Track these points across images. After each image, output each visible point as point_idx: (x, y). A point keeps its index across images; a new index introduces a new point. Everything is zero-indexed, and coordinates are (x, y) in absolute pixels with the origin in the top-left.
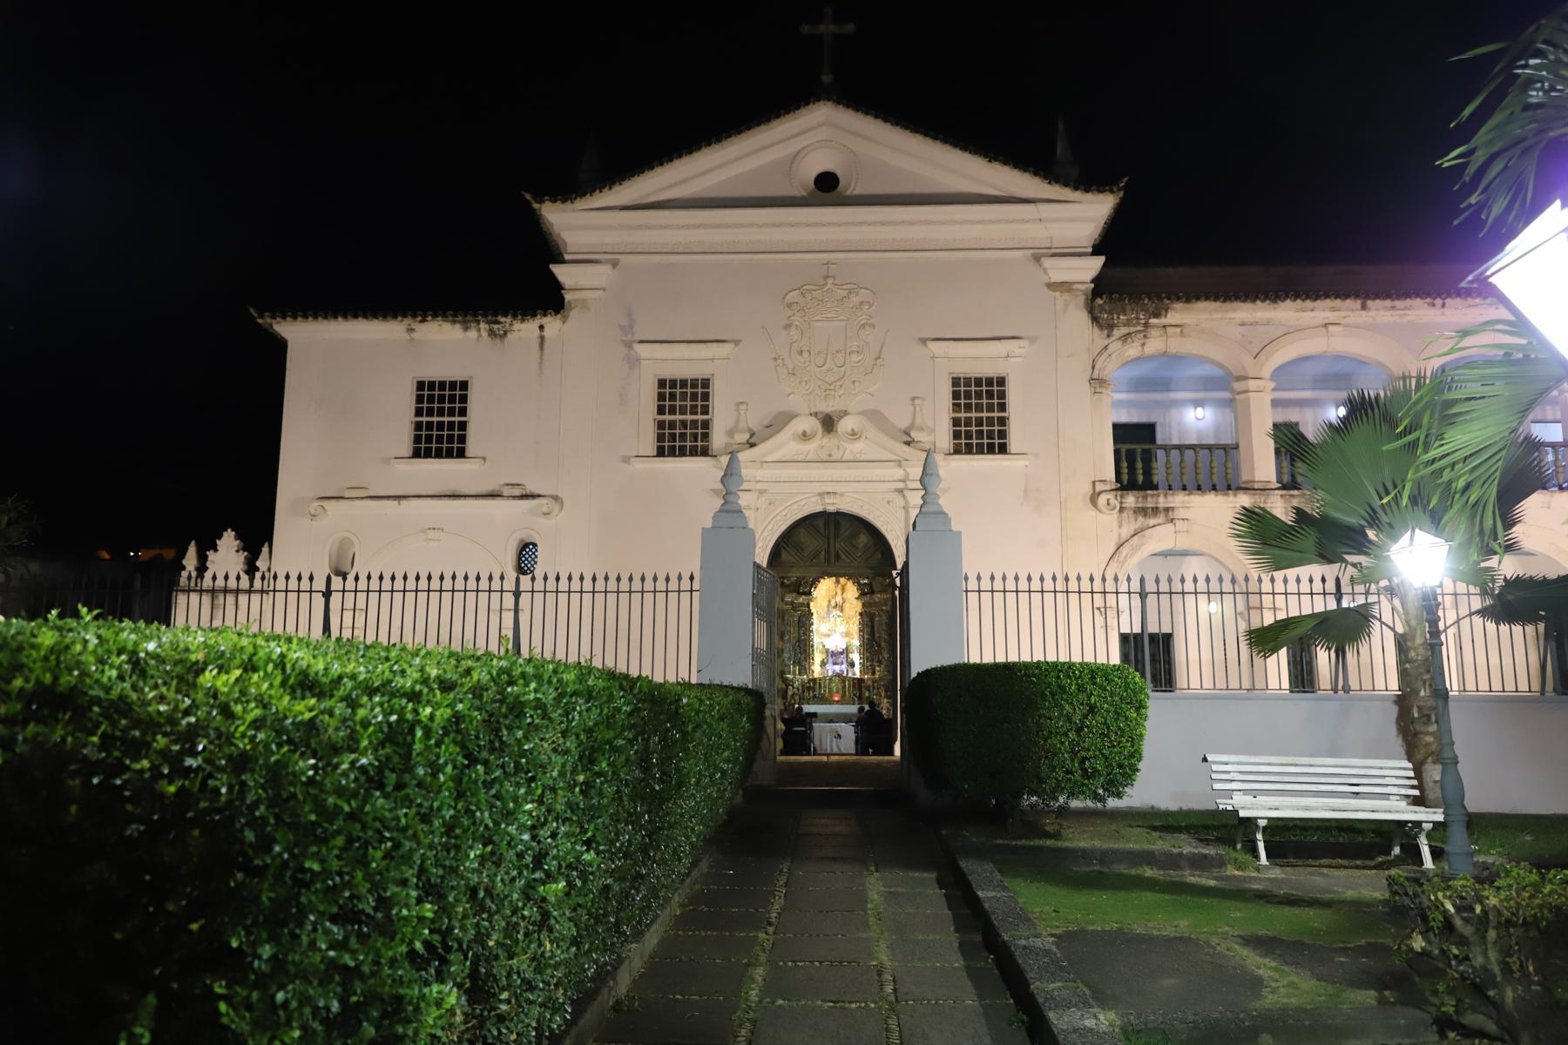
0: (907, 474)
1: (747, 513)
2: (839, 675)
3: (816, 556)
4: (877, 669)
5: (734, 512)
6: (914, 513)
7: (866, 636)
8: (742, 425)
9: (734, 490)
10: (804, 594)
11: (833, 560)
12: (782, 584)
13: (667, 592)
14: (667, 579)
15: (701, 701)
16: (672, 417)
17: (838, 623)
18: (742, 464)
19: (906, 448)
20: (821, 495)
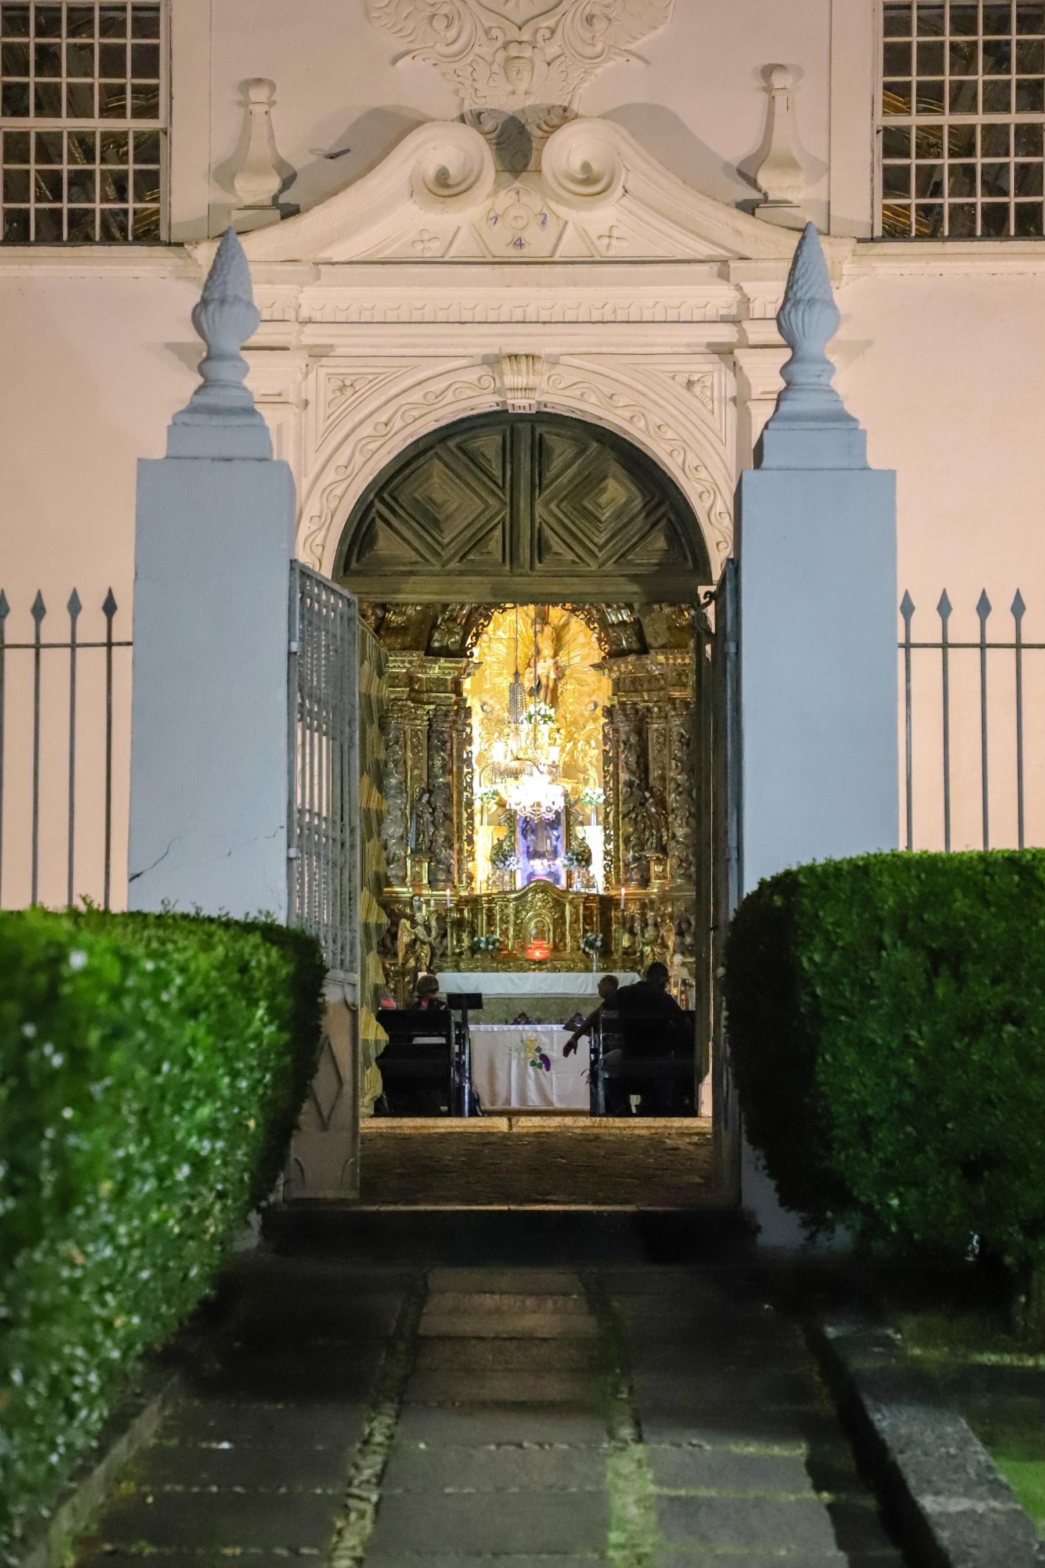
0: (745, 301)
1: (270, 416)
2: (544, 888)
3: (478, 541)
4: (656, 869)
5: (231, 411)
6: (761, 413)
7: (624, 776)
8: (259, 149)
9: (229, 343)
10: (446, 653)
11: (525, 553)
12: (381, 628)
13: (38, 647)
14: (39, 611)
15: (127, 962)
16: (48, 124)
17: (543, 739)
18: (252, 268)
19: (742, 221)
20: (493, 361)
